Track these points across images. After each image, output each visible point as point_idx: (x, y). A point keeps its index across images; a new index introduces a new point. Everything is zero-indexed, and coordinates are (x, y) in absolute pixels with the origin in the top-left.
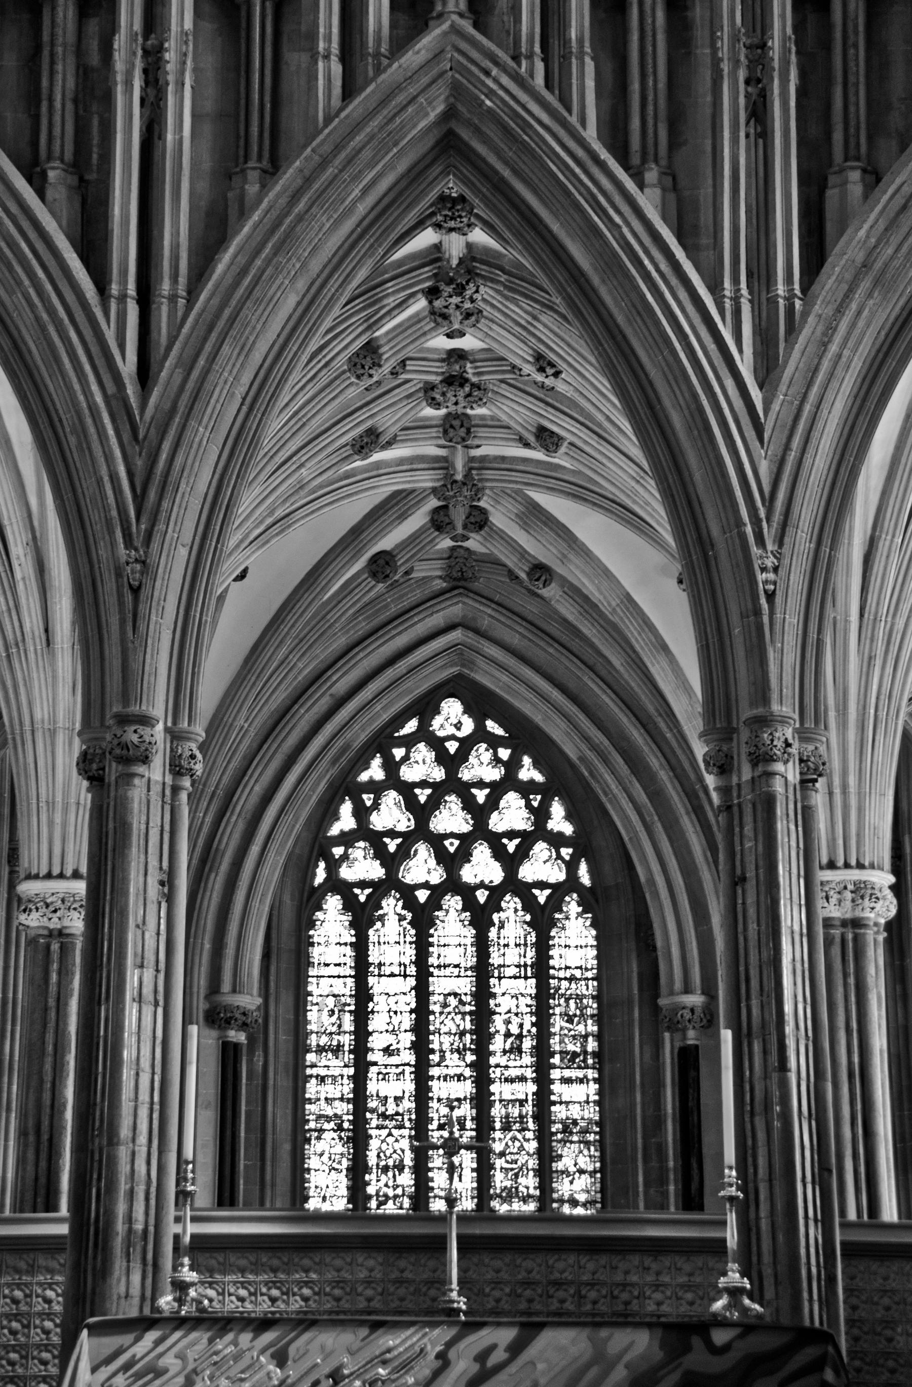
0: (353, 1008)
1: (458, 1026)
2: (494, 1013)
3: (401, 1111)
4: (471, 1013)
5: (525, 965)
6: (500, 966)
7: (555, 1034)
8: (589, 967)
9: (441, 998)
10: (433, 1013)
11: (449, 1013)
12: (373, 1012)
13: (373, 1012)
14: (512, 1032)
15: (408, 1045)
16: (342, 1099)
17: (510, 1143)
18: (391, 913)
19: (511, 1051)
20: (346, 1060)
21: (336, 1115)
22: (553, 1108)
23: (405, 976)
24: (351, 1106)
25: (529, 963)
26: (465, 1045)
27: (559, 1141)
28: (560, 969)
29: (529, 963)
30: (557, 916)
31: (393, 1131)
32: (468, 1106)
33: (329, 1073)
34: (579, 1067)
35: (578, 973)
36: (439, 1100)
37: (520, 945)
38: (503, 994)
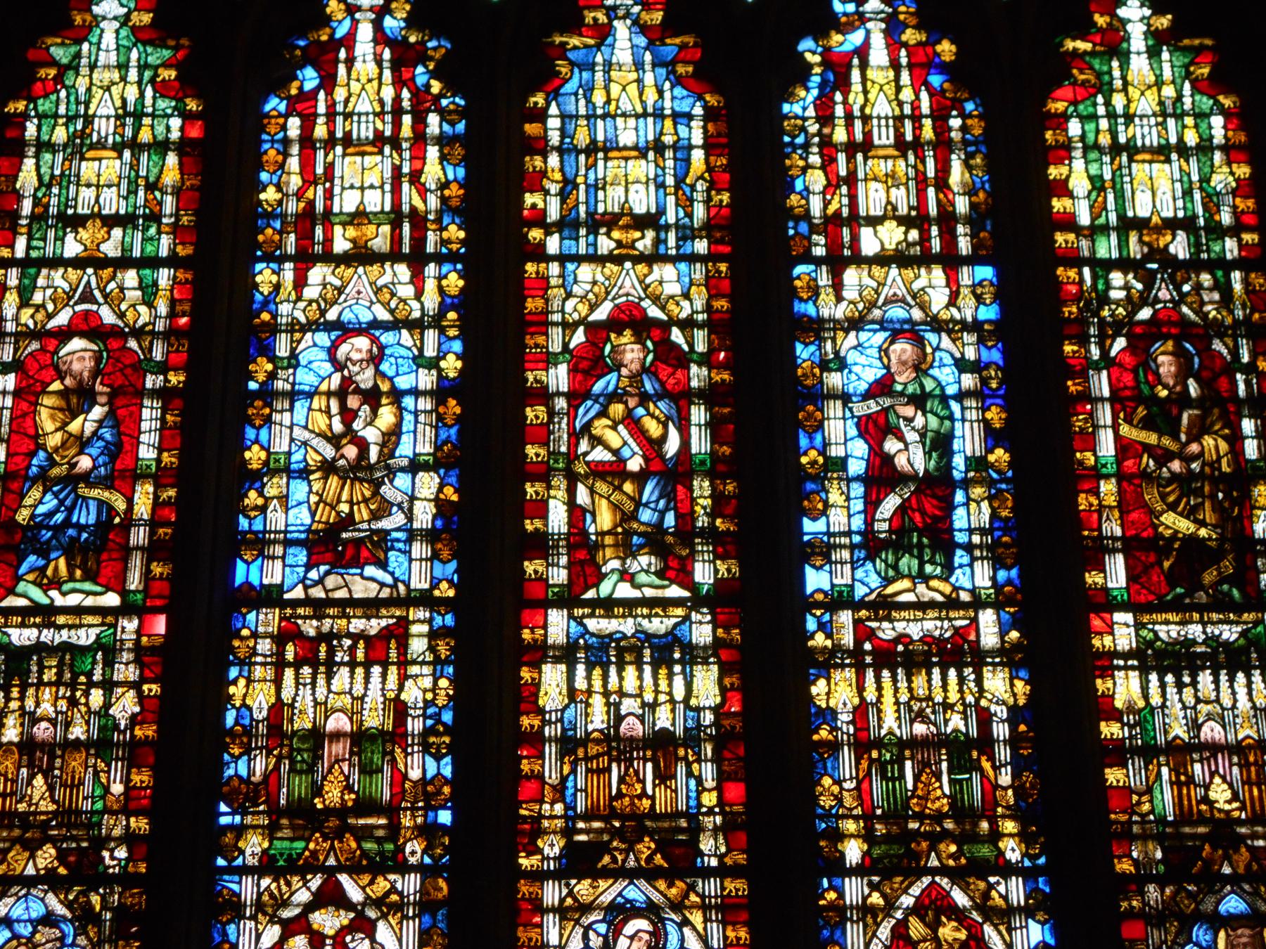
0: (175, 379)
1: (652, 447)
2: (820, 396)
3: (383, 789)
4: (710, 395)
5: (947, 219)
6: (832, 223)
7: (1096, 474)
8: (1226, 218)
9: (579, 337)
10: (543, 395)
11: (614, 397)
12: (267, 394)
13: (267, 394)
14: (901, 462)
15: (424, 515)
16: (101, 746)
17: (916, 929)
18: (365, 32)
19: (899, 541)
20: (134, 581)
21: (67, 815)
22: (1114, 776)
23: (417, 261)
24: (141, 778)
25: (962, 205)
26: (685, 518)
27: (1157, 918)
28: (1095, 231)
29: (962, 205)
30: (1070, 45)
31: (344, 879)
32: (708, 772)
33: (47, 636)
34: (1222, 604)
35: (1179, 247)
36: (569, 745)
37: (917, 145)
38: (855, 324)
